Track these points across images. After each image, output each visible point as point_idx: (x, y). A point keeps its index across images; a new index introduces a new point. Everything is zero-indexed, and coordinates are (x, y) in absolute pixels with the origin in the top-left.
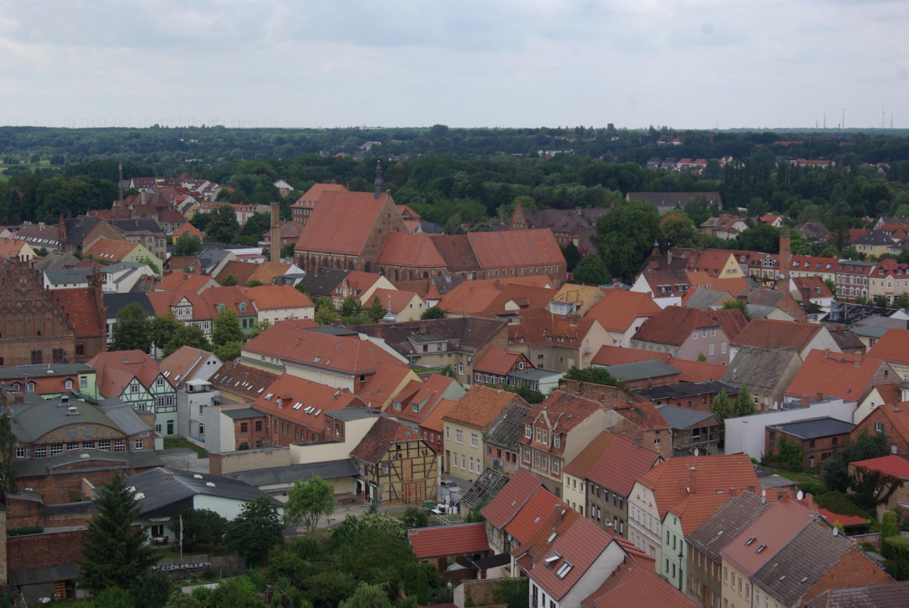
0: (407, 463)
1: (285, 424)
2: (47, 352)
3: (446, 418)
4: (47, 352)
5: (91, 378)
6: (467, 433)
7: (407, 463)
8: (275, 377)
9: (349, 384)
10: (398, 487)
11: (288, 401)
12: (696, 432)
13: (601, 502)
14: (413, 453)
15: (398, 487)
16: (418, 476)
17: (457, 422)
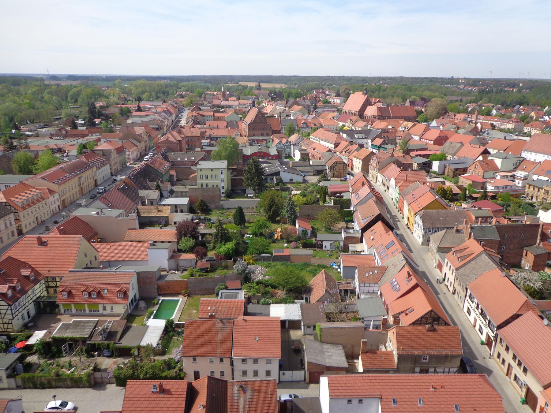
0: (339, 167)
1: (313, 156)
2: (265, 134)
3: (354, 156)
4: (265, 134)
5: (271, 140)
6: (358, 160)
7: (339, 167)
8: (315, 142)
9: (333, 146)
10: (336, 173)
11: (314, 149)
12: (424, 164)
13: (385, 181)
14: (340, 165)
15: (336, 173)
16: (342, 171)
17: (356, 157)
